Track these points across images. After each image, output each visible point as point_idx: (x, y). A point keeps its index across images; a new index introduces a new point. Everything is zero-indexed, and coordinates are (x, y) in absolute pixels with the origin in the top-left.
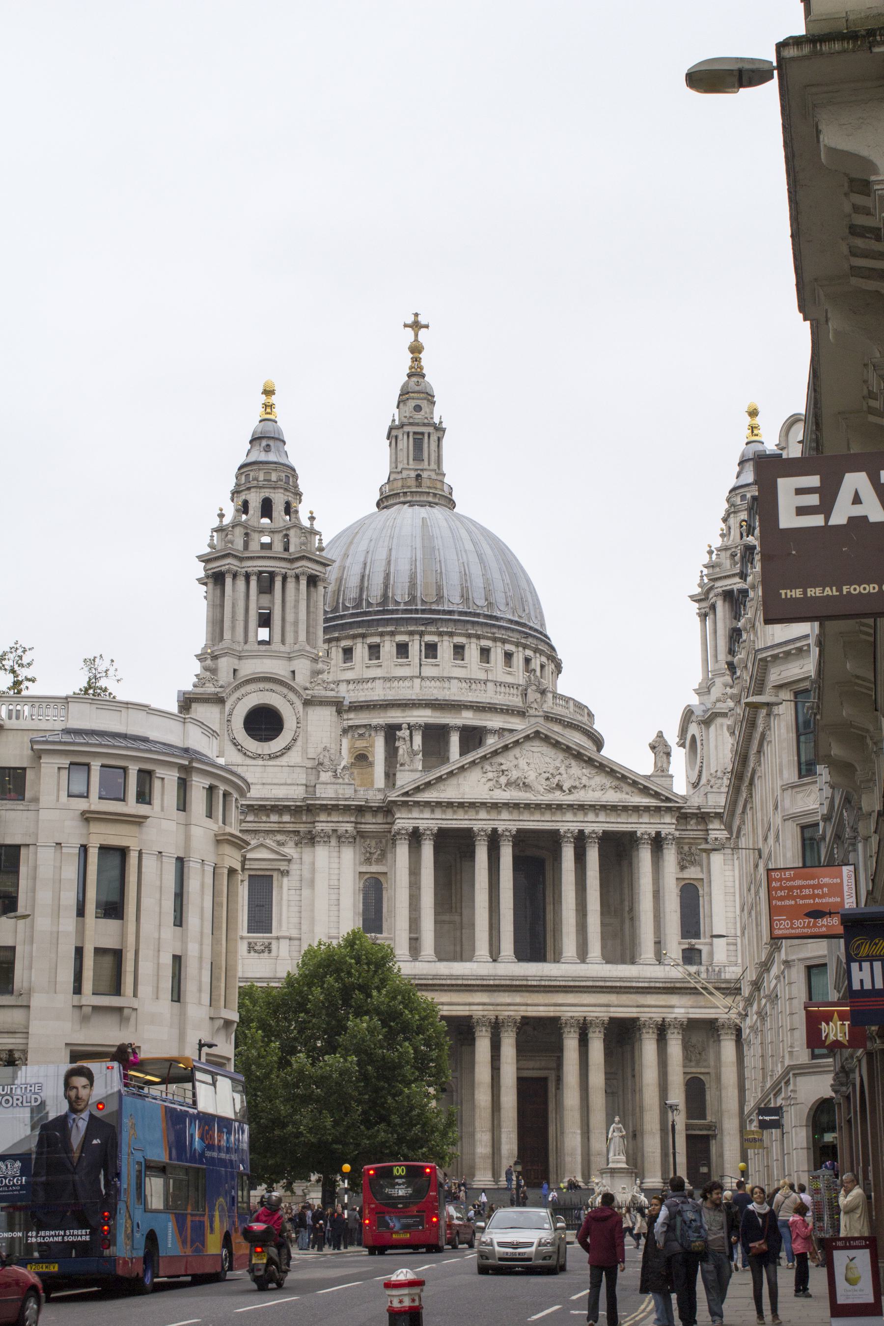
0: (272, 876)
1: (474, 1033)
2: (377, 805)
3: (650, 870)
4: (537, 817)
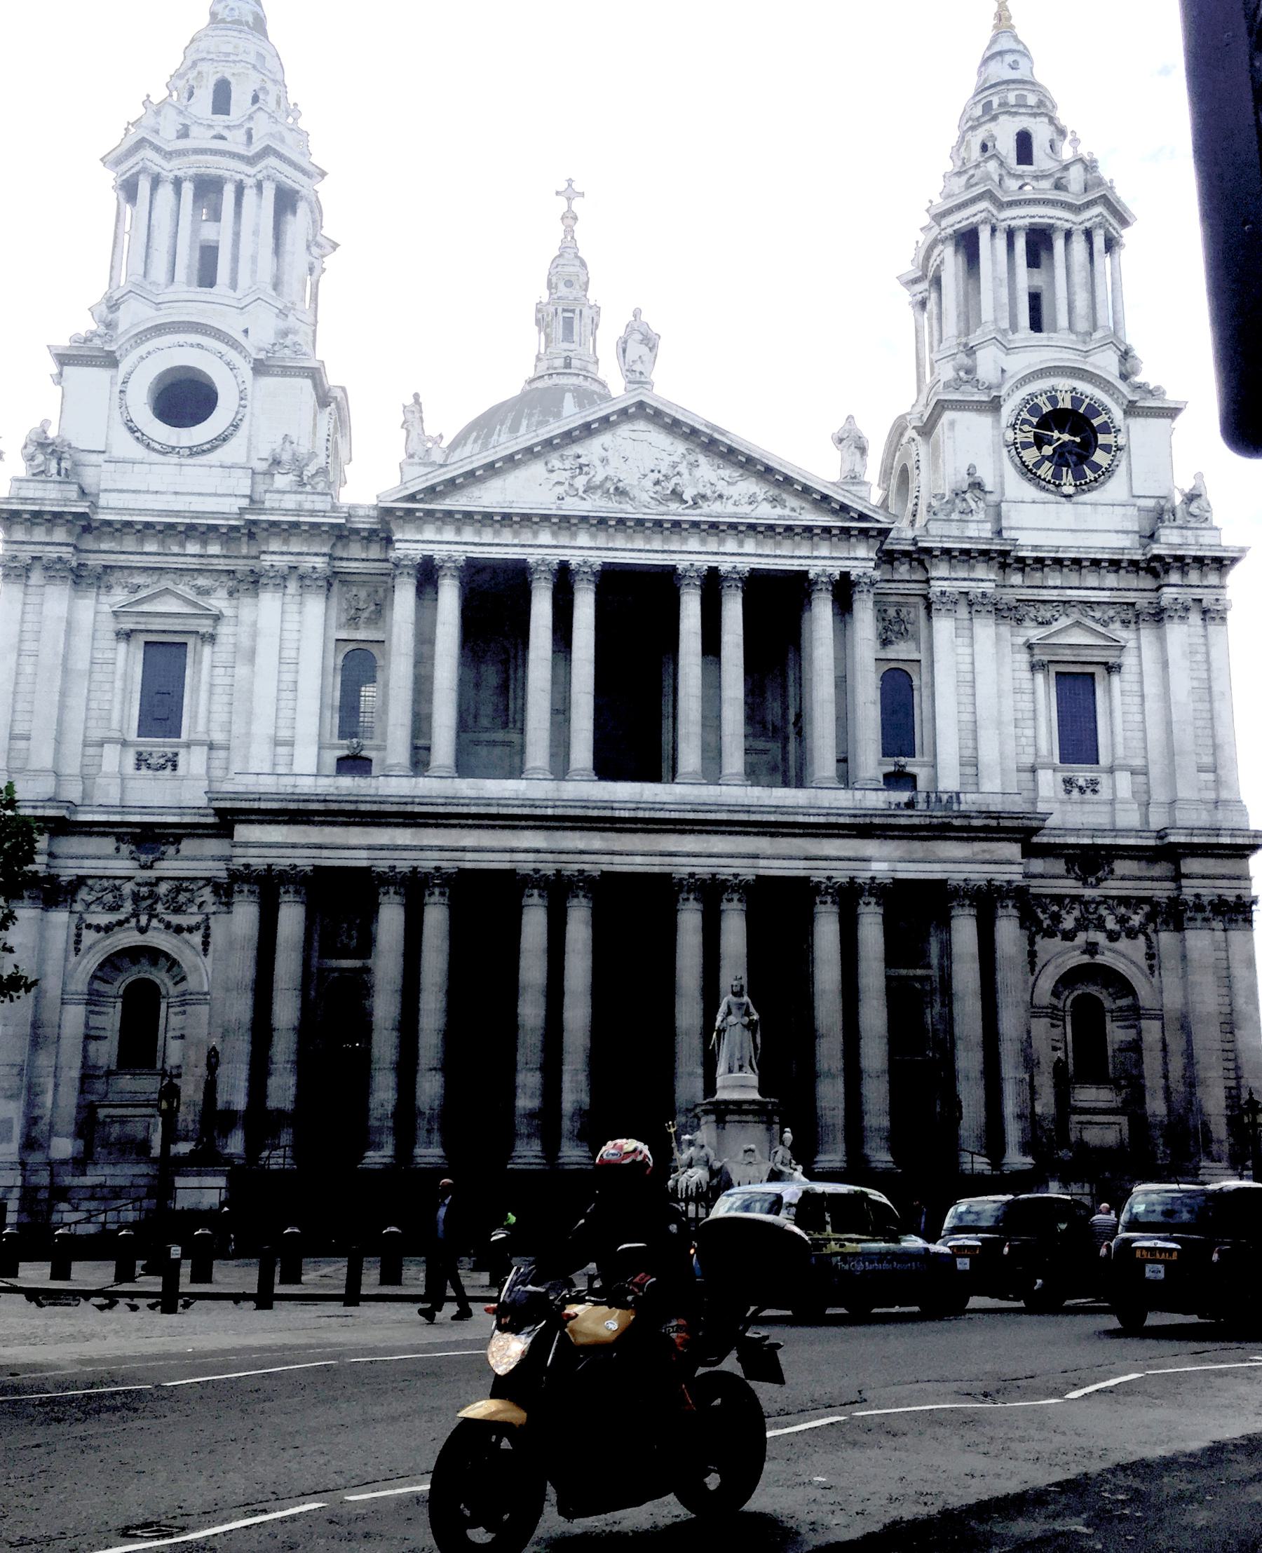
3: (831, 635)
4: (639, 544)
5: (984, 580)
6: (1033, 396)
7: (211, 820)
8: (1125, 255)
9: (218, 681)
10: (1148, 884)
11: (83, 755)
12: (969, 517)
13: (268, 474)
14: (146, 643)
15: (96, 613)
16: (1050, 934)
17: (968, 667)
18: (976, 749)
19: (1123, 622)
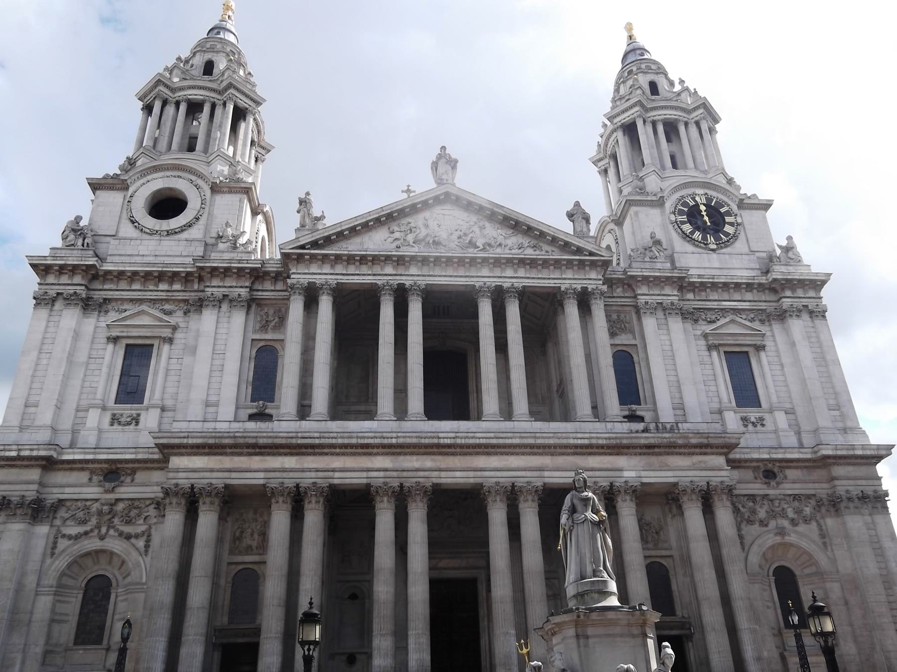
0: (153, 345)
1: (373, 508)
2: (275, 269)
4: (450, 272)
5: (671, 295)
6: (683, 197)
7: (156, 457)
8: (719, 137)
9: (171, 367)
11: (76, 417)
12: (656, 260)
13: (215, 245)
14: (127, 345)
15: (96, 327)
17: (668, 348)
18: (681, 398)
19: (760, 320)
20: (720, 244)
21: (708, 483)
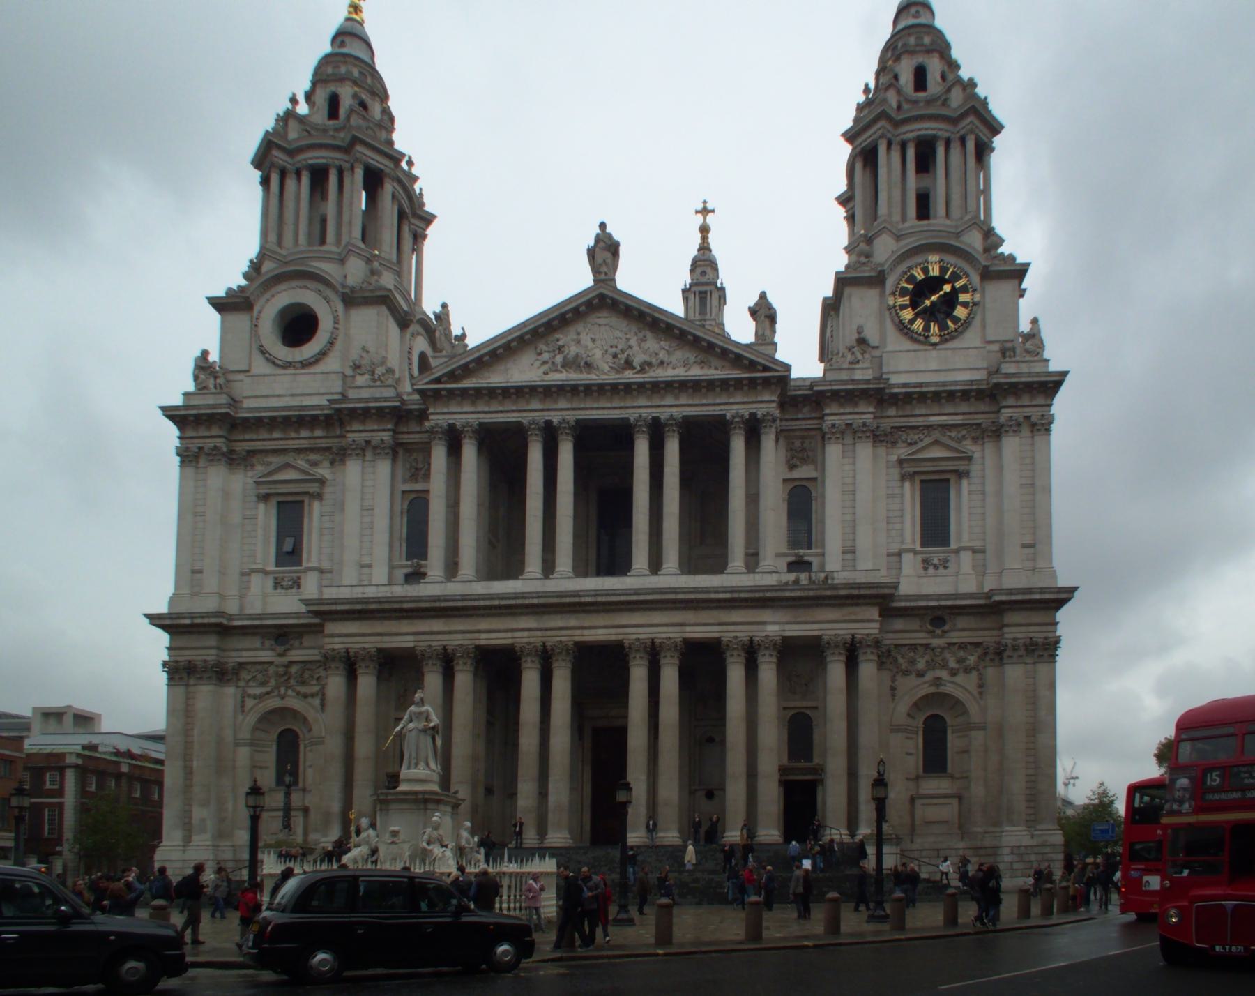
0: (302, 502)
1: (520, 665)
5: (864, 414)
7: (316, 621)
10: (981, 633)
12: (857, 366)
16: (906, 673)
20: (944, 335)
21: (853, 636)
